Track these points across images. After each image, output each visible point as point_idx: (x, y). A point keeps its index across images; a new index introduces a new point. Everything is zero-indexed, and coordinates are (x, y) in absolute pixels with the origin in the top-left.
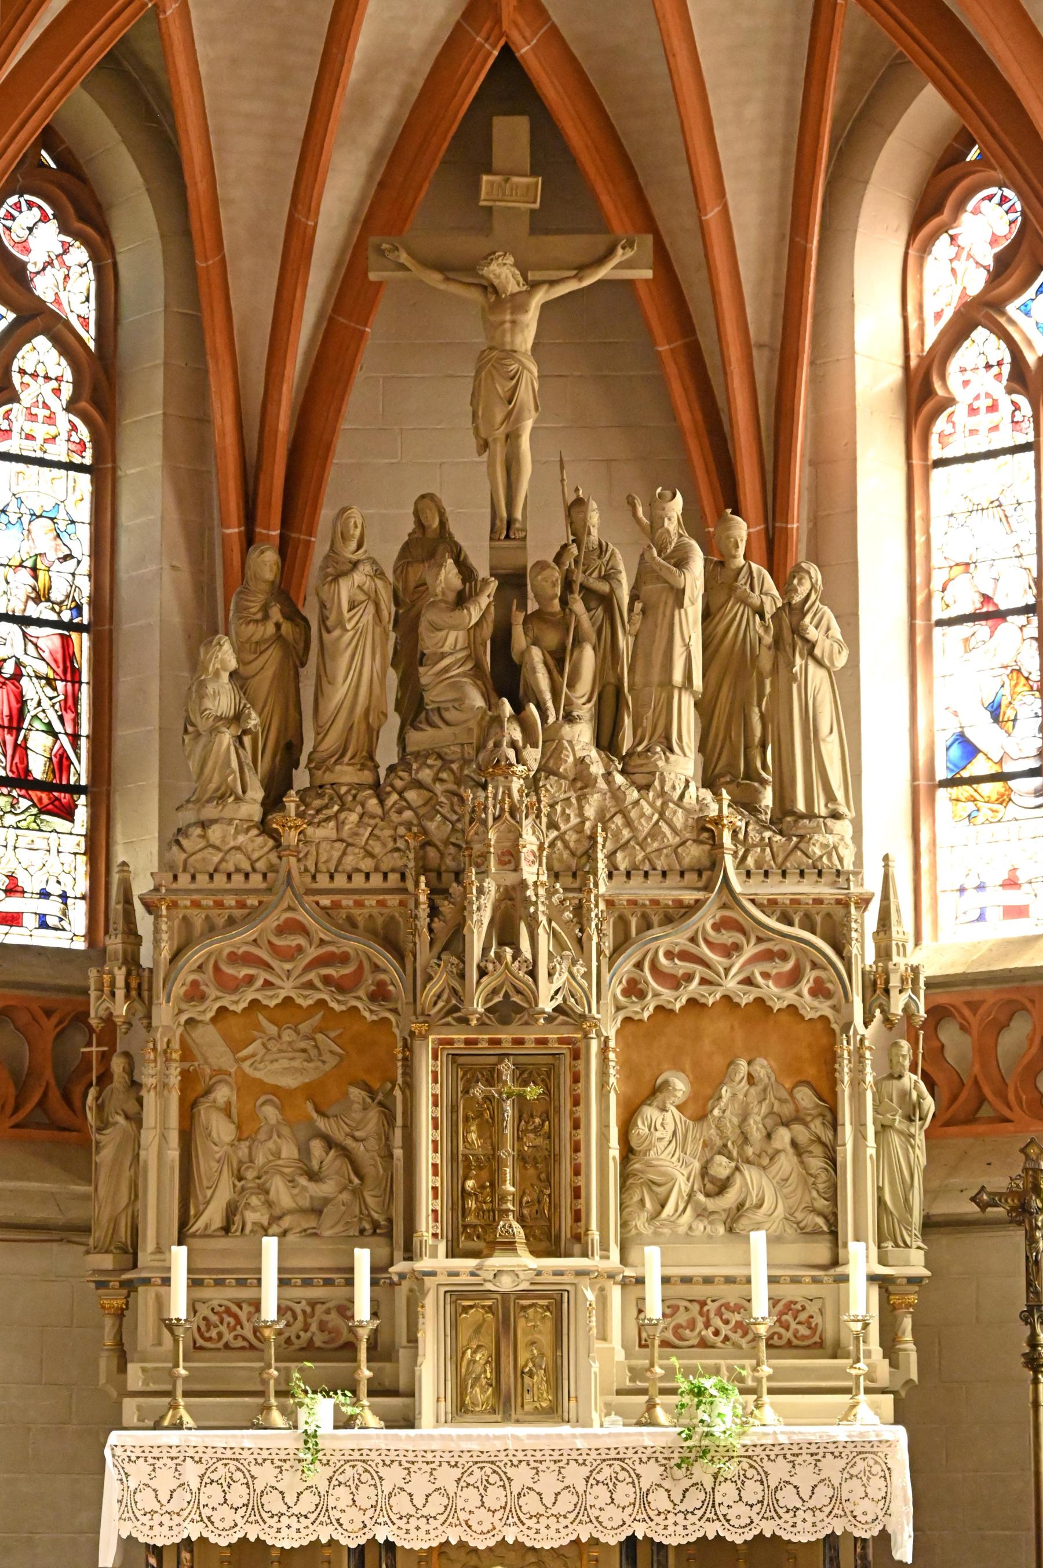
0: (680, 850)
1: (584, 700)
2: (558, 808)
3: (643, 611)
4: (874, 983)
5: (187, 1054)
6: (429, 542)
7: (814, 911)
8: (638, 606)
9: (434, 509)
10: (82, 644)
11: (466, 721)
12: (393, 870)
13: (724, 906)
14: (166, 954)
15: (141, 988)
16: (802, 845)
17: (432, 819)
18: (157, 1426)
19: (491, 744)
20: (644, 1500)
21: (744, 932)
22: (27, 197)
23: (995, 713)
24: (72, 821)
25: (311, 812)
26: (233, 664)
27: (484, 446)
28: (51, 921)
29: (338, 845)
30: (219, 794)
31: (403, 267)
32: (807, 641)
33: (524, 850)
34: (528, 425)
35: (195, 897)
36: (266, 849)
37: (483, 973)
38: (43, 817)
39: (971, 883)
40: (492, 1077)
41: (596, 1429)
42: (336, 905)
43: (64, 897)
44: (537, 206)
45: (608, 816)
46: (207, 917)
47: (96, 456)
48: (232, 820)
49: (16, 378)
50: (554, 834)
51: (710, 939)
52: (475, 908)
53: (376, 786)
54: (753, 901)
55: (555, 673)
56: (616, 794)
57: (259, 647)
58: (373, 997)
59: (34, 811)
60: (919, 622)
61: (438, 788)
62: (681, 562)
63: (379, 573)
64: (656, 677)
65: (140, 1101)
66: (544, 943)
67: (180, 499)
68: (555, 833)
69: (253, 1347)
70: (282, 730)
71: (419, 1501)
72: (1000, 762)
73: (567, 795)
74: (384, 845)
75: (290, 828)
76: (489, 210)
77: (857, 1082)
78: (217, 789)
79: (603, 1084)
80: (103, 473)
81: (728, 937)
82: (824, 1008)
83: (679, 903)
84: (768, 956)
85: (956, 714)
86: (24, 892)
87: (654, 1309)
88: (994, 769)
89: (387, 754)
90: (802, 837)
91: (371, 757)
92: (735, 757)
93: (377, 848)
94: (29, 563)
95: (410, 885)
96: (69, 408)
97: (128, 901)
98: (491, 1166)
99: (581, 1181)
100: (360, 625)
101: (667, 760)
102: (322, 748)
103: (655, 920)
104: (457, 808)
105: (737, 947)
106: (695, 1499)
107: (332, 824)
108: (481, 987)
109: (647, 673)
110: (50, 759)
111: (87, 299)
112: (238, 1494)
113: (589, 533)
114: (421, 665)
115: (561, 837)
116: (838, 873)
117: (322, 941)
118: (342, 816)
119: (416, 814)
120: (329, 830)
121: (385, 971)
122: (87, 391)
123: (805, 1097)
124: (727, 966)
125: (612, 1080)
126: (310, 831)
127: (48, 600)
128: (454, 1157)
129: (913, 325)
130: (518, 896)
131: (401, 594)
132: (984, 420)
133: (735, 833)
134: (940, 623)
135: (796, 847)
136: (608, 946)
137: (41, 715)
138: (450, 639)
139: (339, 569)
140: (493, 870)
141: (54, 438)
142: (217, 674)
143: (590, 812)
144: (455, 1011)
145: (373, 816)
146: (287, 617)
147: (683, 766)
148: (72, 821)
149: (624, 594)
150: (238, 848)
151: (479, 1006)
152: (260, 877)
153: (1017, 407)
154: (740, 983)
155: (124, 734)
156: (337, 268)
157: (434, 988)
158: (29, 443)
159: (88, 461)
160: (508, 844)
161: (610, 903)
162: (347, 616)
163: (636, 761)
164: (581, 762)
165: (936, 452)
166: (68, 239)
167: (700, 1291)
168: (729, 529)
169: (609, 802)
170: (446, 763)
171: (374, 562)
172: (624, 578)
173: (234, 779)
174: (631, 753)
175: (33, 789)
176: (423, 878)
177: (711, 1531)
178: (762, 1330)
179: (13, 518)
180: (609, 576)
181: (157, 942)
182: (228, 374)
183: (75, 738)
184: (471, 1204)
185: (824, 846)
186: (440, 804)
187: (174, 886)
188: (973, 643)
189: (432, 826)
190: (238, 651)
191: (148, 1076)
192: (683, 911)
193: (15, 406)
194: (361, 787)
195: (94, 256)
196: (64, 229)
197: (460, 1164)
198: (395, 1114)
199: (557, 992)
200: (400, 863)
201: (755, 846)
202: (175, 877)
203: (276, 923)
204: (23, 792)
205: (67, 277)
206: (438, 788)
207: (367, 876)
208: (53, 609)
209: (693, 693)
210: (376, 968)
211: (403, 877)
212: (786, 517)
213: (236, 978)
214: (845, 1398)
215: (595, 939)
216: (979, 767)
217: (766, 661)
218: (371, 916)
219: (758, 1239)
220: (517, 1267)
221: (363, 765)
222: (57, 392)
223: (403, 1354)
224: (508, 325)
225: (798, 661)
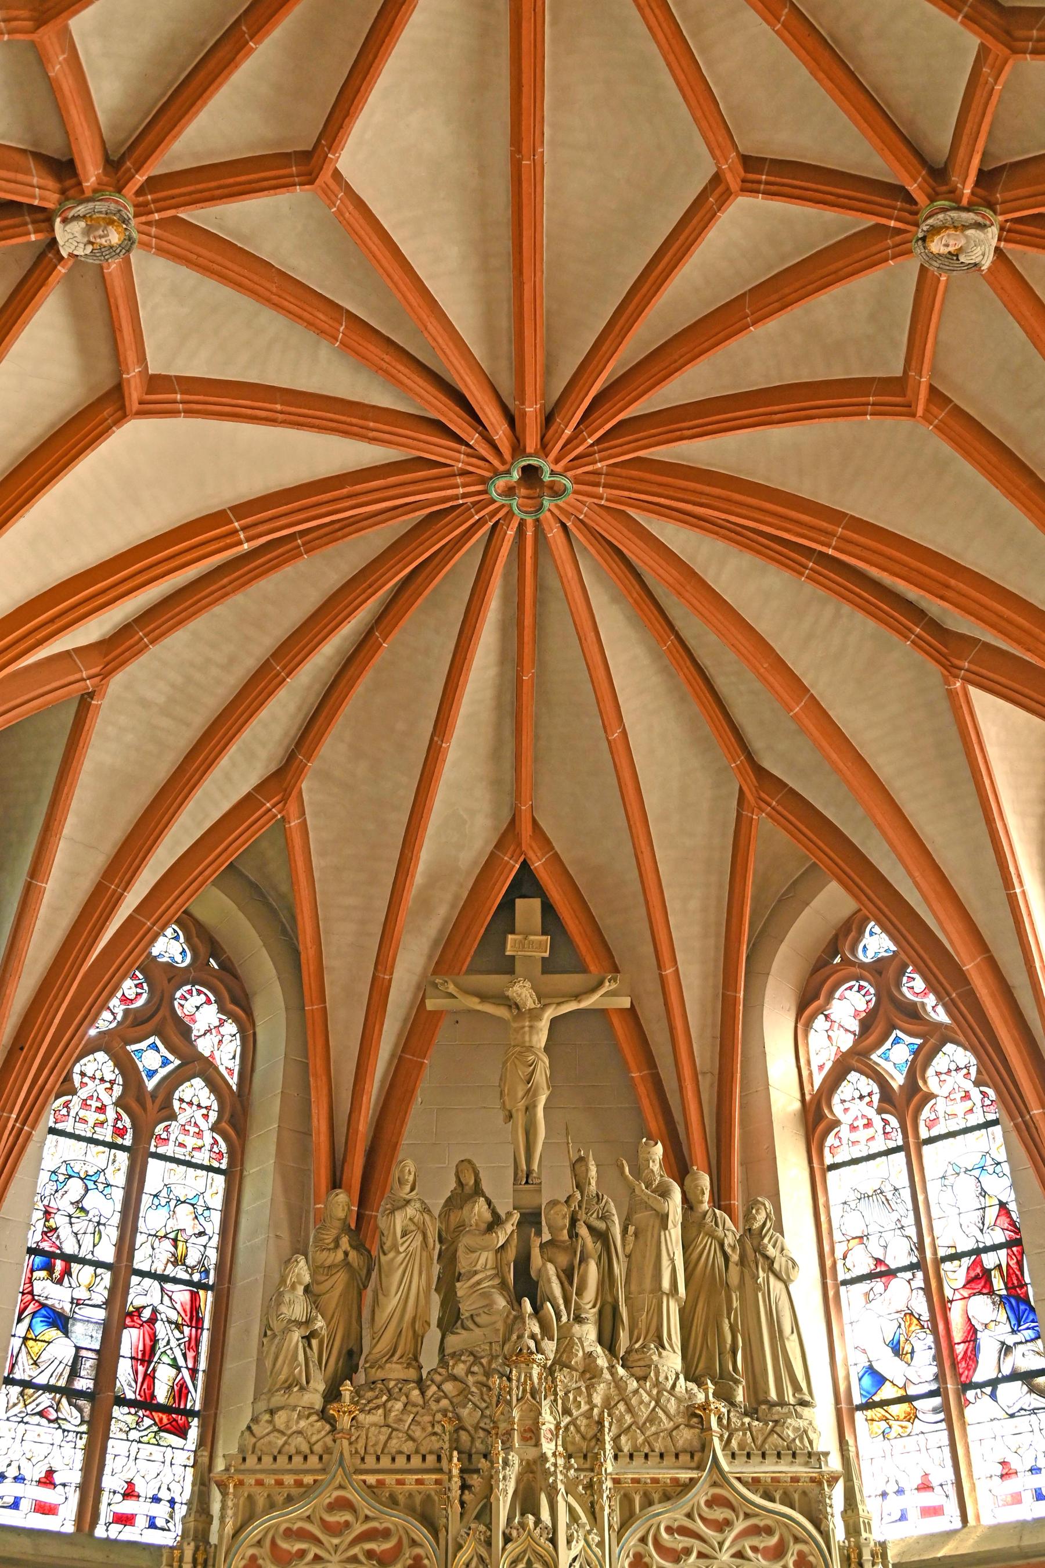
0: (674, 1433)
1: (590, 1305)
2: (571, 1396)
4: (849, 1558)
6: (468, 1191)
7: (792, 1490)
9: (471, 1170)
10: (207, 1299)
11: (495, 1323)
12: (431, 1452)
13: (715, 1484)
14: (229, 1529)
16: (778, 1429)
17: (465, 1407)
19: (514, 1337)
21: (733, 1509)
22: (197, 987)
23: (897, 1350)
24: (185, 1439)
25: (364, 1401)
28: (160, 1523)
29: (386, 1428)
30: (286, 1385)
31: (452, 996)
32: (767, 1257)
33: (544, 1427)
34: (542, 1100)
35: (259, 1476)
36: (323, 1433)
37: (507, 1539)
38: (162, 1434)
39: (891, 1488)
42: (381, 1483)
43: (172, 1502)
44: (547, 955)
45: (612, 1404)
46: (269, 1496)
47: (229, 1164)
48: (296, 1406)
49: (176, 1104)
50: (567, 1419)
51: (705, 1515)
52: (501, 1477)
53: (420, 1383)
54: (739, 1479)
55: (566, 1283)
56: (618, 1384)
59: (155, 1429)
60: (829, 1282)
61: (471, 1379)
62: (664, 1193)
63: (426, 1210)
64: (648, 1284)
66: (563, 1517)
67: (286, 1190)
68: (569, 1419)
70: (346, 1336)
72: (904, 1387)
73: (578, 1385)
74: (424, 1429)
75: (344, 1413)
76: (513, 957)
78: (286, 1381)
81: (720, 1514)
83: (675, 1481)
84: (755, 1531)
85: (864, 1351)
86: (139, 1496)
88: (900, 1393)
89: (429, 1360)
90: (776, 1422)
91: (416, 1359)
92: (711, 1359)
93: (418, 1433)
94: (172, 1236)
95: (444, 1463)
96: (213, 1129)
100: (411, 1249)
101: (660, 1354)
102: (375, 1351)
103: (656, 1497)
104: (486, 1397)
105: (728, 1523)
107: (380, 1411)
108: (506, 1553)
109: (640, 1283)
110: (173, 1387)
111: (234, 1058)
113: (590, 1184)
114: (458, 1281)
115: (573, 1422)
116: (810, 1455)
117: (367, 1518)
118: (389, 1404)
119: (451, 1403)
120: (377, 1417)
121: (421, 1546)
122: (227, 1116)
124: (720, 1539)
126: (361, 1417)
127: (184, 1264)
129: (805, 1073)
130: (538, 1469)
131: (444, 1234)
132: (862, 1134)
133: (720, 1419)
134: (845, 1283)
135: (772, 1431)
136: (616, 1520)
137: (169, 1352)
138: (481, 1261)
140: (517, 1445)
141: (200, 1148)
142: (293, 1287)
143: (597, 1399)
145: (415, 1405)
147: (672, 1362)
148: (185, 1439)
149: (617, 1231)
150: (300, 1432)
152: (316, 1459)
153: (886, 1122)
154: (733, 1556)
155: (231, 1366)
156: (406, 1020)
157: (463, 1556)
158: (182, 1150)
159: (224, 1166)
160: (531, 1422)
161: (616, 1481)
162: (400, 1241)
163: (635, 1356)
166: (224, 1018)
168: (697, 1179)
169: (613, 1391)
170: (477, 1359)
171: (423, 1203)
172: (616, 1219)
173: (300, 1371)
174: (628, 1352)
175: (156, 1411)
176: (455, 1453)
179: (163, 1202)
180: (604, 1217)
181: (222, 1518)
182: (325, 1091)
183: (194, 1372)
185: (796, 1429)
186: (472, 1393)
187: (243, 1467)
188: (872, 1296)
189: (465, 1412)
192: (680, 1489)
193: (174, 1123)
195: (242, 1030)
196: (221, 1010)
199: (574, 1560)
200: (436, 1446)
201: (737, 1430)
202: (244, 1459)
203: (328, 1500)
204: (148, 1413)
205: (220, 1041)
206: (471, 1379)
207: (409, 1458)
208: (187, 1271)
209: (677, 1300)
210: (414, 1543)
213: (289, 1552)
215: (607, 1511)
216: (887, 1392)
218: (410, 1494)
221: (408, 1364)
222: (206, 1116)
224: (527, 1029)
225: (761, 1274)
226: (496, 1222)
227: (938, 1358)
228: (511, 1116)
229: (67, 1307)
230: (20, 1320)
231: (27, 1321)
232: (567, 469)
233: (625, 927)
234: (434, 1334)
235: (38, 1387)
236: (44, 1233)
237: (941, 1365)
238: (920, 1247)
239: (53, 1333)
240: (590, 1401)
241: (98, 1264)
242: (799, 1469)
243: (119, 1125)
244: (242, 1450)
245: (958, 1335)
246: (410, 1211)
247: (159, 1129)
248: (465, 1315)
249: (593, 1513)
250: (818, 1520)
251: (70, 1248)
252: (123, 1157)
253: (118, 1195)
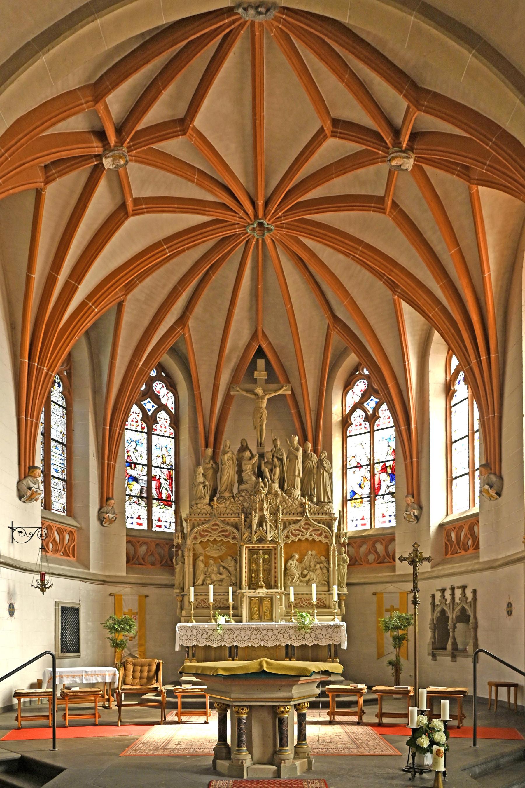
3: (289, 461)
5: (194, 550)
6: (244, 448)
8: (288, 459)
10: (173, 473)
13: (306, 520)
14: (189, 530)
15: (184, 537)
18: (188, 622)
20: (290, 637)
23: (360, 485)
26: (203, 472)
27: (256, 428)
34: (265, 423)
37: (256, 532)
40: (258, 554)
41: (280, 623)
42: (225, 520)
49: (158, 419)
53: (233, 497)
56: (284, 498)
57: (208, 469)
58: (233, 538)
61: (246, 497)
63: (233, 454)
64: (292, 474)
65: (184, 559)
66: (269, 527)
67: (192, 443)
69: (208, 608)
70: (213, 486)
71: (243, 637)
77: (334, 555)
79: (281, 555)
80: (177, 439)
81: (307, 527)
82: (327, 541)
83: (297, 520)
84: (315, 530)
87: (292, 599)
89: (235, 491)
91: (232, 491)
92: (308, 491)
93: (233, 509)
95: (240, 516)
97: (181, 520)
98: (257, 572)
99: (276, 574)
105: (309, 529)
106: (301, 637)
112: (205, 636)
115: (272, 506)
120: (223, 505)
122: (173, 422)
123: (323, 558)
125: (283, 555)
128: (250, 570)
133: (308, 506)
134: (349, 468)
138: (248, 467)
139: (225, 453)
142: (199, 474)
143: (278, 501)
144: (250, 541)
146: (214, 463)
147: (298, 492)
151: (255, 539)
157: (245, 536)
159: (173, 436)
161: (282, 520)
163: (288, 491)
164: (276, 491)
165: (348, 435)
167: (300, 596)
170: (247, 492)
174: (286, 490)
177: (304, 643)
178: (315, 603)
180: (281, 455)
181: (187, 528)
184: (253, 579)
190: (204, 470)
191: (186, 554)
194: (230, 497)
197: (251, 571)
198: (238, 562)
206: (246, 497)
210: (233, 533)
211: (239, 515)
212: (318, 446)
214: (333, 617)
217: (315, 471)
219: (314, 586)
220: (263, 592)
222: (166, 422)
223: (239, 608)
226: (252, 456)
227: (370, 488)
228: (256, 428)
229: (137, 476)
232: (273, 223)
233: (290, 364)
234: (236, 485)
235: (133, 496)
237: (371, 490)
238: (370, 460)
239: (134, 483)
240: (276, 501)
241: (143, 465)
242: (327, 517)
243: (143, 426)
244: (190, 512)
245: (377, 482)
246: (229, 454)
247: (154, 427)
248: (244, 481)
249: (276, 527)
250: (330, 527)
251: (135, 461)
252: (145, 435)
253: (145, 445)
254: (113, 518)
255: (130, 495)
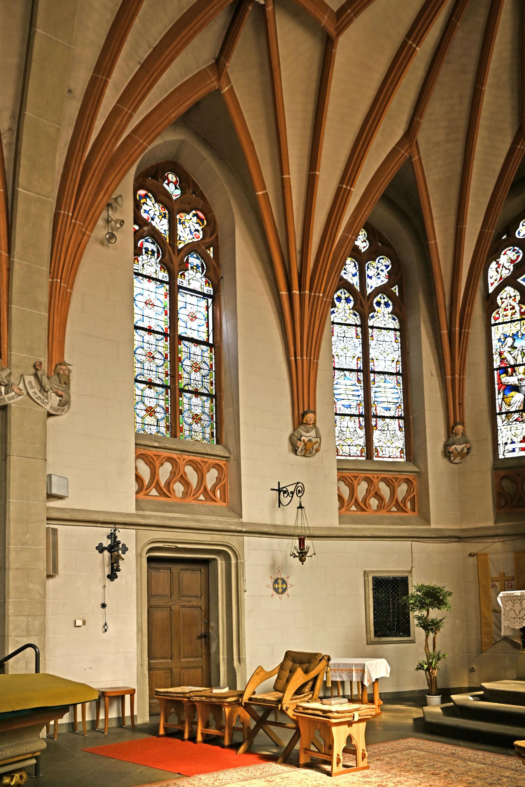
229: (517, 383)
230: (499, 393)
231: (502, 394)
235: (512, 412)
236: (500, 361)
239: (513, 393)
251: (512, 363)
254: (463, 449)
255: (508, 413)
